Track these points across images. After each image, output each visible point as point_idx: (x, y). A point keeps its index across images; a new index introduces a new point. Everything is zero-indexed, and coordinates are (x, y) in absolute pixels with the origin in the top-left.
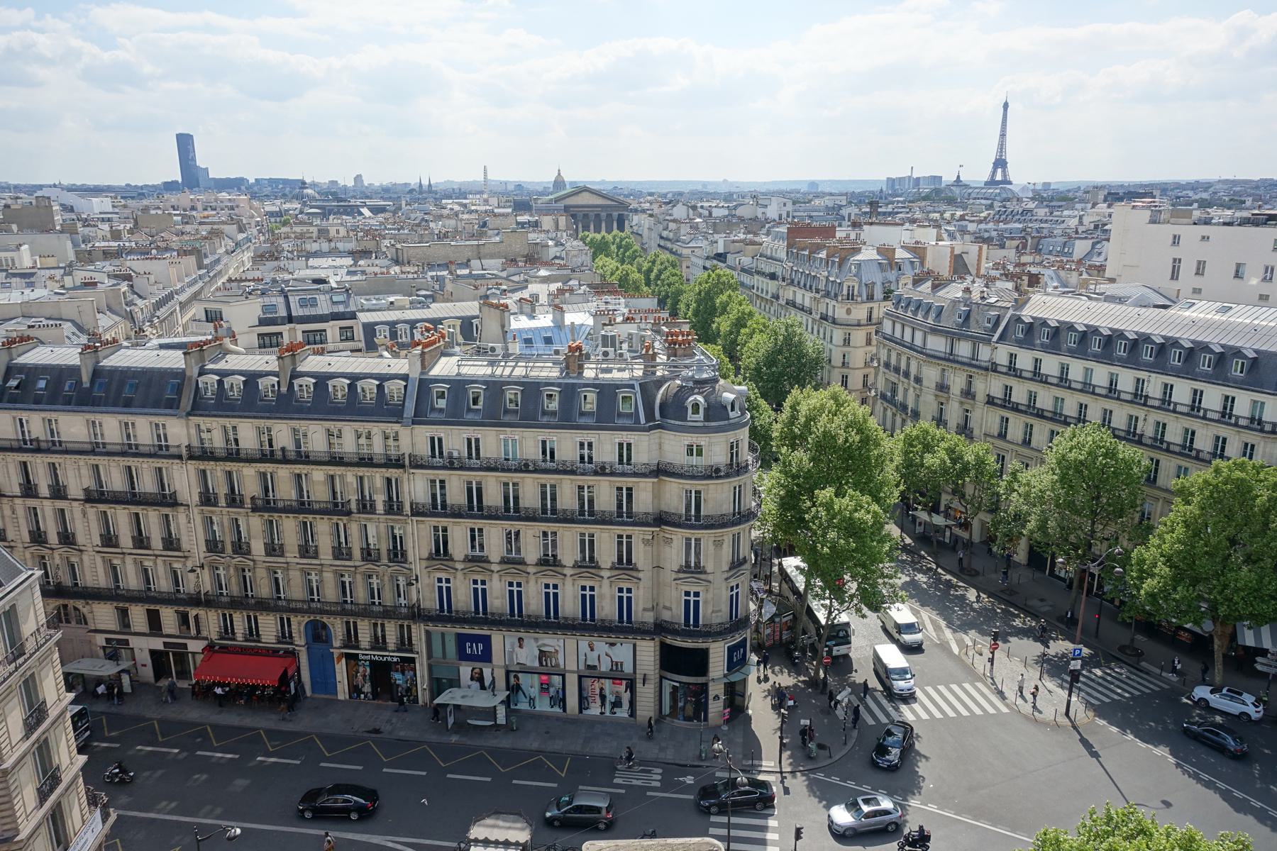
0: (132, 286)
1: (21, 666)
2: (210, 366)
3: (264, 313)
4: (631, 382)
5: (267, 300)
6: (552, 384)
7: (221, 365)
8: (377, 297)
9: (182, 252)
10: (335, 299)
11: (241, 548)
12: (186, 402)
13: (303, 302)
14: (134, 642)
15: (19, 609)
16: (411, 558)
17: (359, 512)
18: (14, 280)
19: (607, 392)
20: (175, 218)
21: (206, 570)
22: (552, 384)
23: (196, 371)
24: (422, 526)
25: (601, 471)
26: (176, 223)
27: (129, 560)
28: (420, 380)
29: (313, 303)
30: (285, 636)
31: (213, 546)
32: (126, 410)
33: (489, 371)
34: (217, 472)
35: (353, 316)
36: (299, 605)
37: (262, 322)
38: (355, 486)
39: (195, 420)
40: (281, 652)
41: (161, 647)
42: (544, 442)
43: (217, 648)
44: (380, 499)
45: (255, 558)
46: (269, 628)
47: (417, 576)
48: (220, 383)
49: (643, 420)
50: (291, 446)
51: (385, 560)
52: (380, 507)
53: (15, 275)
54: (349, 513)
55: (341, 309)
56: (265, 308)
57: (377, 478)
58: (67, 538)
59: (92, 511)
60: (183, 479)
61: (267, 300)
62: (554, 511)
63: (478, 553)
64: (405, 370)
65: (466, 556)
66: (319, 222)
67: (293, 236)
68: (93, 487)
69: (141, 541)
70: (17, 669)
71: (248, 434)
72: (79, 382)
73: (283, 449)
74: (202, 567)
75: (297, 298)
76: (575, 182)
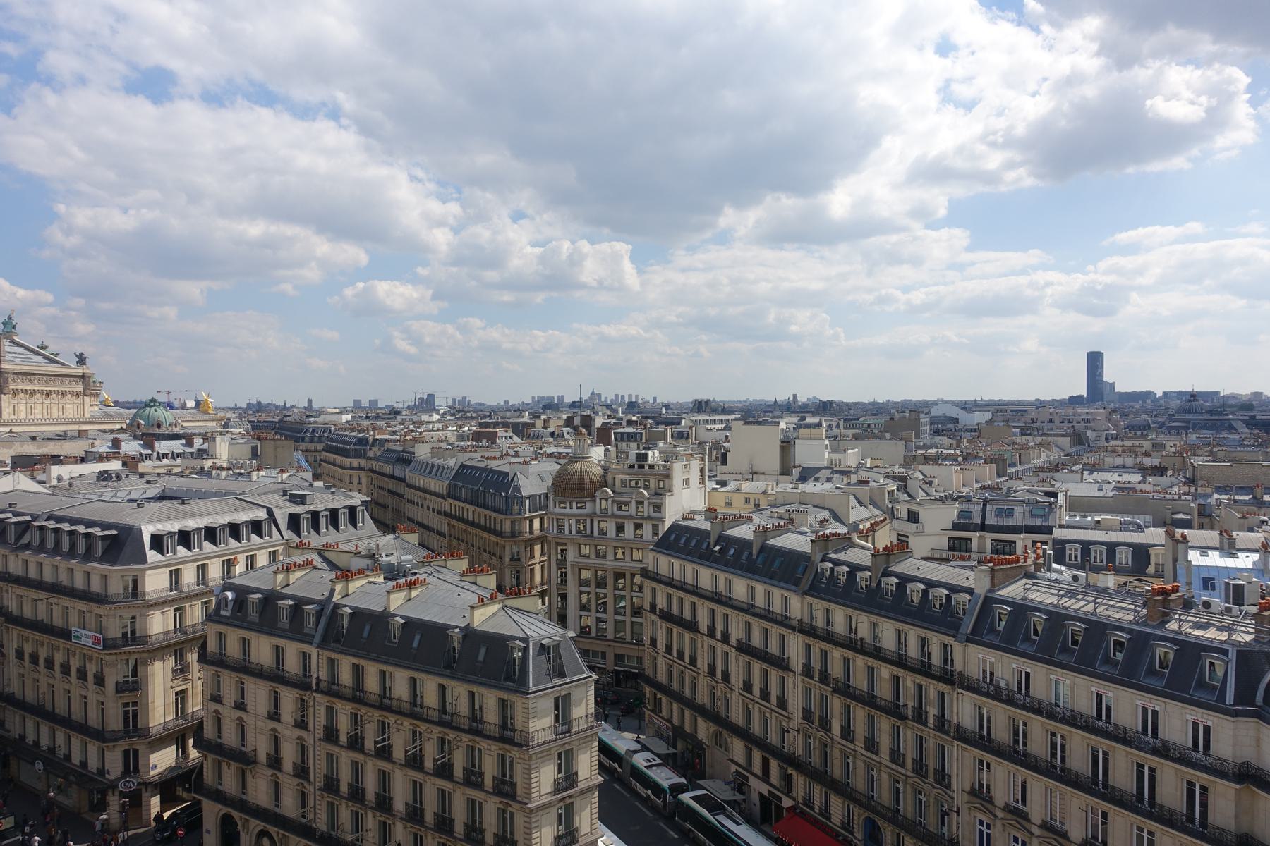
0: (905, 486)
1: (560, 739)
2: (832, 556)
3: (959, 518)
4: (1225, 647)
5: (966, 507)
6: (1122, 629)
7: (841, 556)
8: (1083, 514)
9: (988, 460)
10: (1035, 512)
11: (825, 724)
12: (806, 583)
13: (999, 513)
14: (753, 782)
15: (573, 698)
16: (954, 787)
17: (913, 720)
18: (835, 475)
19: (1190, 652)
20: (1014, 430)
21: (801, 735)
22: (1122, 629)
23: (819, 557)
24: (966, 754)
25: (1165, 751)
26: (1014, 434)
27: (757, 705)
28: (986, 598)
29: (1010, 513)
30: (847, 826)
31: (807, 714)
32: (769, 581)
33: (1054, 600)
34: (817, 646)
35: (1049, 531)
36: (858, 796)
37: (956, 527)
38: (912, 692)
39: (809, 599)
40: (841, 838)
41: (766, 793)
42: (1099, 696)
43: (798, 811)
44: (932, 712)
45: (834, 737)
46: (837, 808)
47: (958, 808)
48: (832, 570)
49: (1230, 698)
50: (868, 640)
51: (932, 780)
52: (931, 721)
53: (837, 472)
54: (903, 718)
55: (1039, 522)
56: (962, 514)
57: (932, 689)
58: (726, 677)
59: (743, 658)
60: (795, 647)
61: (966, 507)
62: (1106, 785)
63: (1020, 805)
64: (970, 584)
65: (1007, 805)
66: (1154, 436)
67: (1120, 449)
68: (744, 640)
69: (765, 695)
70: (556, 740)
71: (839, 616)
72: (751, 554)
73: (862, 639)
74: (798, 731)
75: (995, 507)
76: (259, 407)
